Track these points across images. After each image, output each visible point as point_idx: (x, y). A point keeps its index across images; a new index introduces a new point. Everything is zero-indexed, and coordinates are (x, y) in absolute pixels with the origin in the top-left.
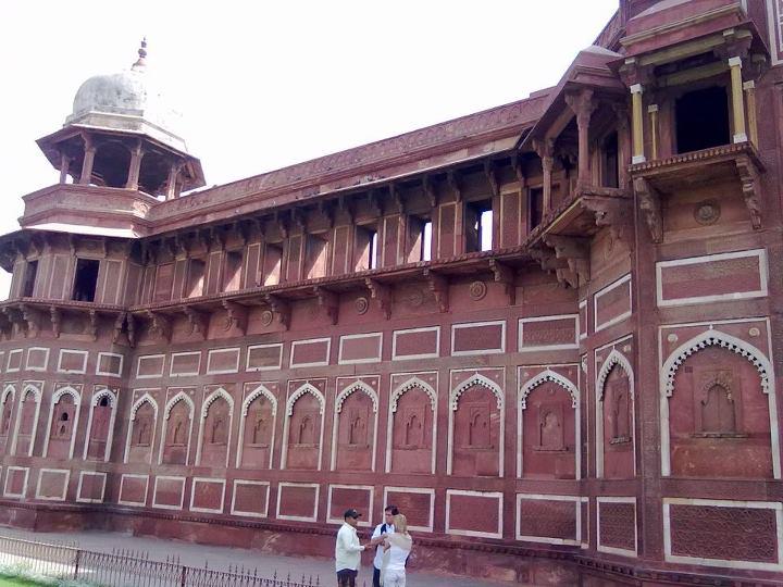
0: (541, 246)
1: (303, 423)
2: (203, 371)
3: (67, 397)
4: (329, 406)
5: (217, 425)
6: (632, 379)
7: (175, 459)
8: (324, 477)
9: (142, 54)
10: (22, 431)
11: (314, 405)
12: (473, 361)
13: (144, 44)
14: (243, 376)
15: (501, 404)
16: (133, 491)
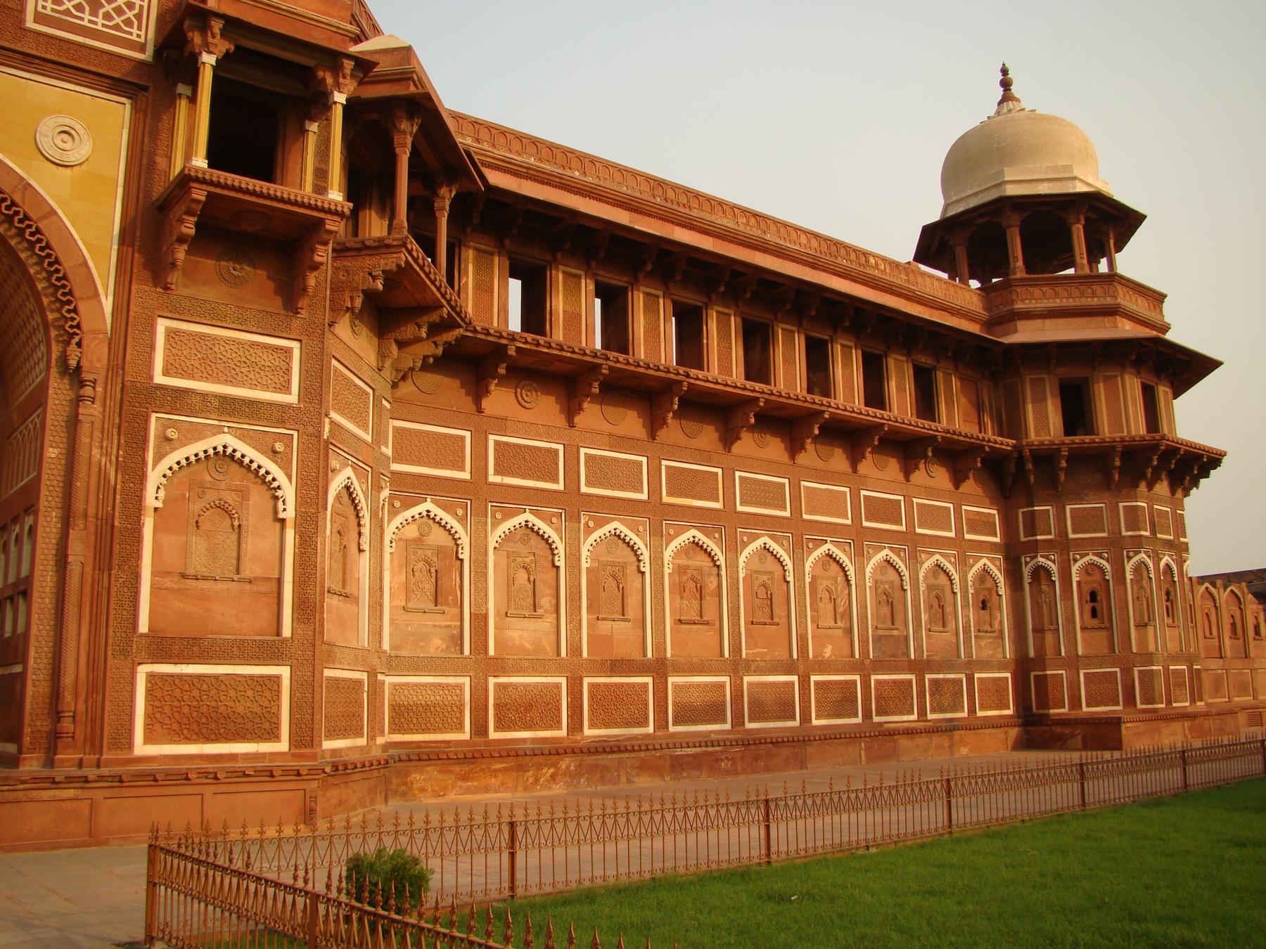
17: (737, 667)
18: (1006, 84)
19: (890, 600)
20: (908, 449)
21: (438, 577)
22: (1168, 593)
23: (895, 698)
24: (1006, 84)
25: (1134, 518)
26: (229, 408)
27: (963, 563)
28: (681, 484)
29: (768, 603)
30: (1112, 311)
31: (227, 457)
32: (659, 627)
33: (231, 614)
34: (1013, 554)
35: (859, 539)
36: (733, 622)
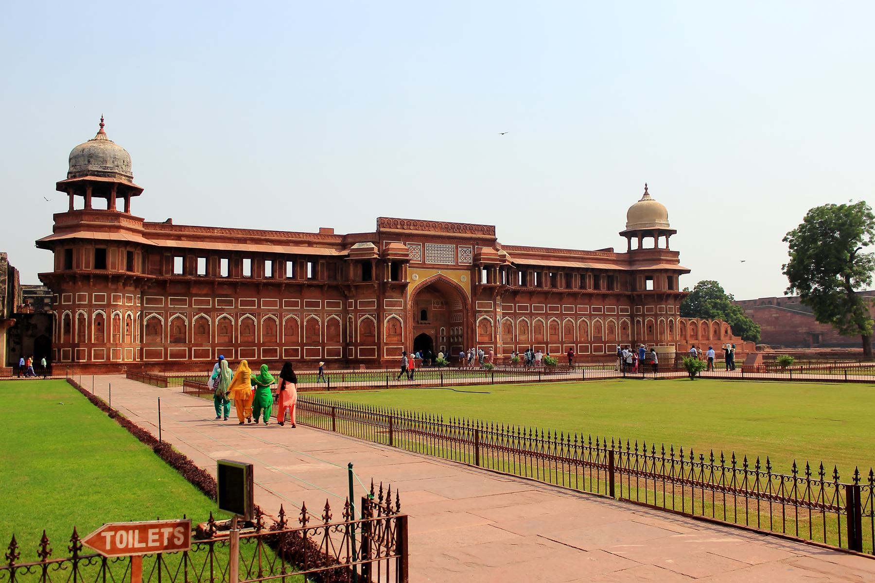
0: (348, 287)
1: (248, 326)
2: (190, 305)
3: (129, 315)
4: (259, 322)
5: (203, 327)
6: (376, 322)
7: (176, 340)
8: (259, 345)
9: (102, 125)
10: (114, 330)
11: (250, 321)
12: (312, 311)
13: (102, 120)
14: (214, 309)
15: (320, 323)
16: (150, 354)
17: (562, 343)
18: (646, 189)
19: (598, 329)
20: (604, 296)
21: (508, 329)
22: (671, 327)
23: (598, 349)
24: (646, 189)
25: (661, 309)
26: (486, 312)
27: (618, 320)
28: (551, 309)
29: (569, 330)
30: (659, 261)
31: (485, 319)
32: (547, 336)
33: (486, 339)
34: (632, 317)
35: (590, 316)
36: (562, 334)
